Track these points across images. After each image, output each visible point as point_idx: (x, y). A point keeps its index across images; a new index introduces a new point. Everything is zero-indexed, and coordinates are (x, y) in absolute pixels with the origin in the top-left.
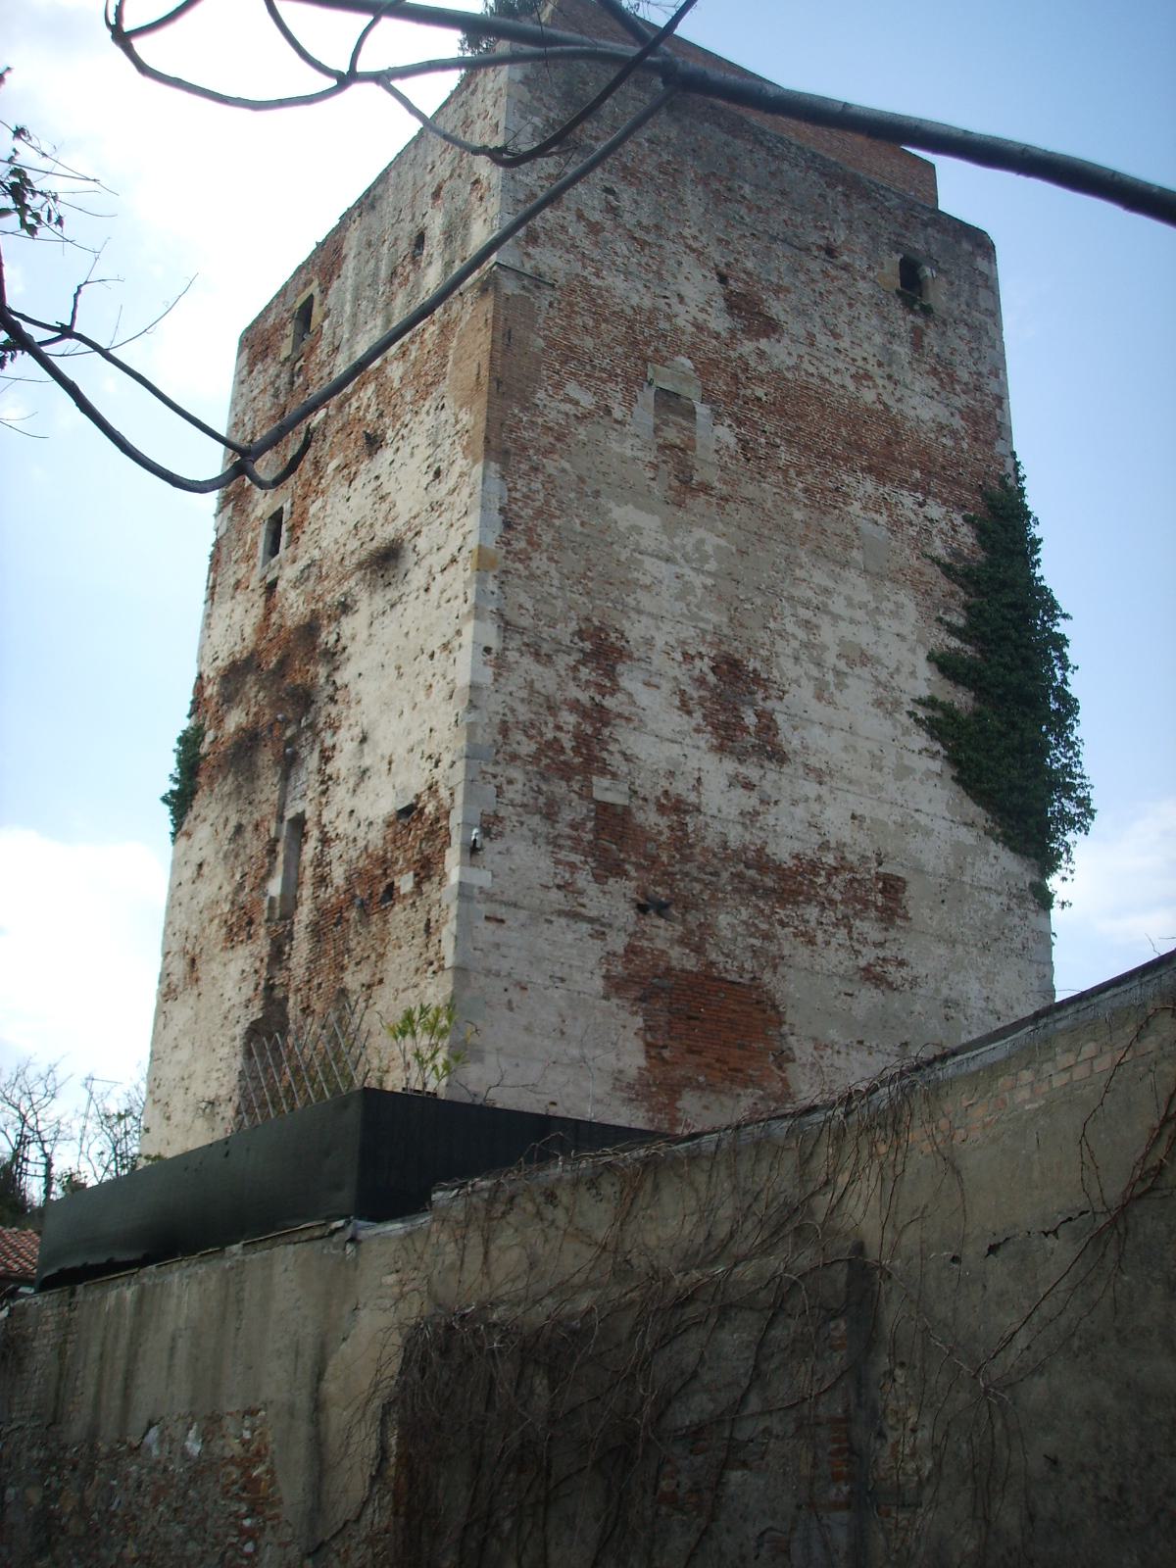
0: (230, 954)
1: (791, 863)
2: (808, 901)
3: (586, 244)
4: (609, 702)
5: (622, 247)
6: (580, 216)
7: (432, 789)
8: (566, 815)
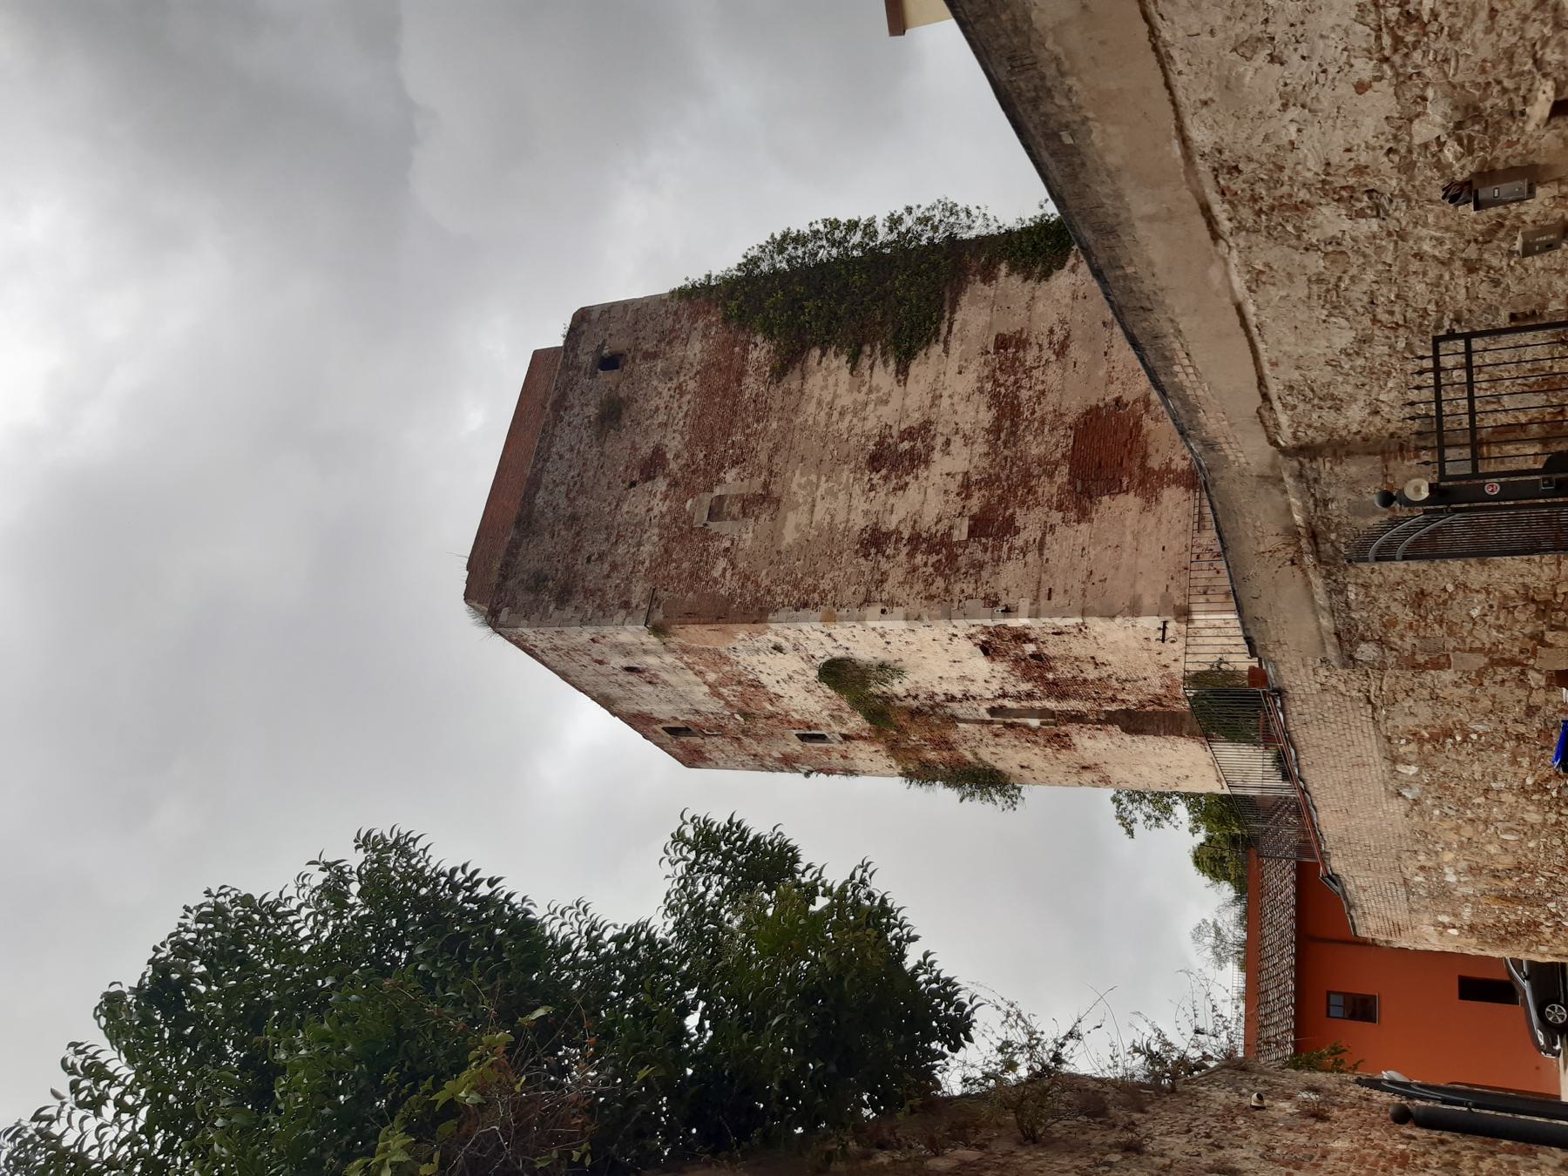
0: (1079, 746)
1: (994, 411)
2: (1017, 397)
3: (624, 572)
4: (906, 535)
5: (621, 549)
6: (608, 576)
7: (970, 637)
8: (979, 555)
